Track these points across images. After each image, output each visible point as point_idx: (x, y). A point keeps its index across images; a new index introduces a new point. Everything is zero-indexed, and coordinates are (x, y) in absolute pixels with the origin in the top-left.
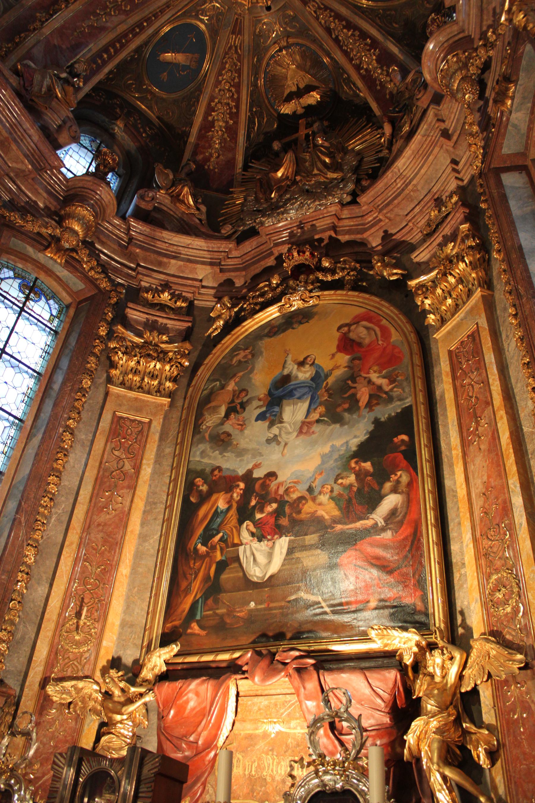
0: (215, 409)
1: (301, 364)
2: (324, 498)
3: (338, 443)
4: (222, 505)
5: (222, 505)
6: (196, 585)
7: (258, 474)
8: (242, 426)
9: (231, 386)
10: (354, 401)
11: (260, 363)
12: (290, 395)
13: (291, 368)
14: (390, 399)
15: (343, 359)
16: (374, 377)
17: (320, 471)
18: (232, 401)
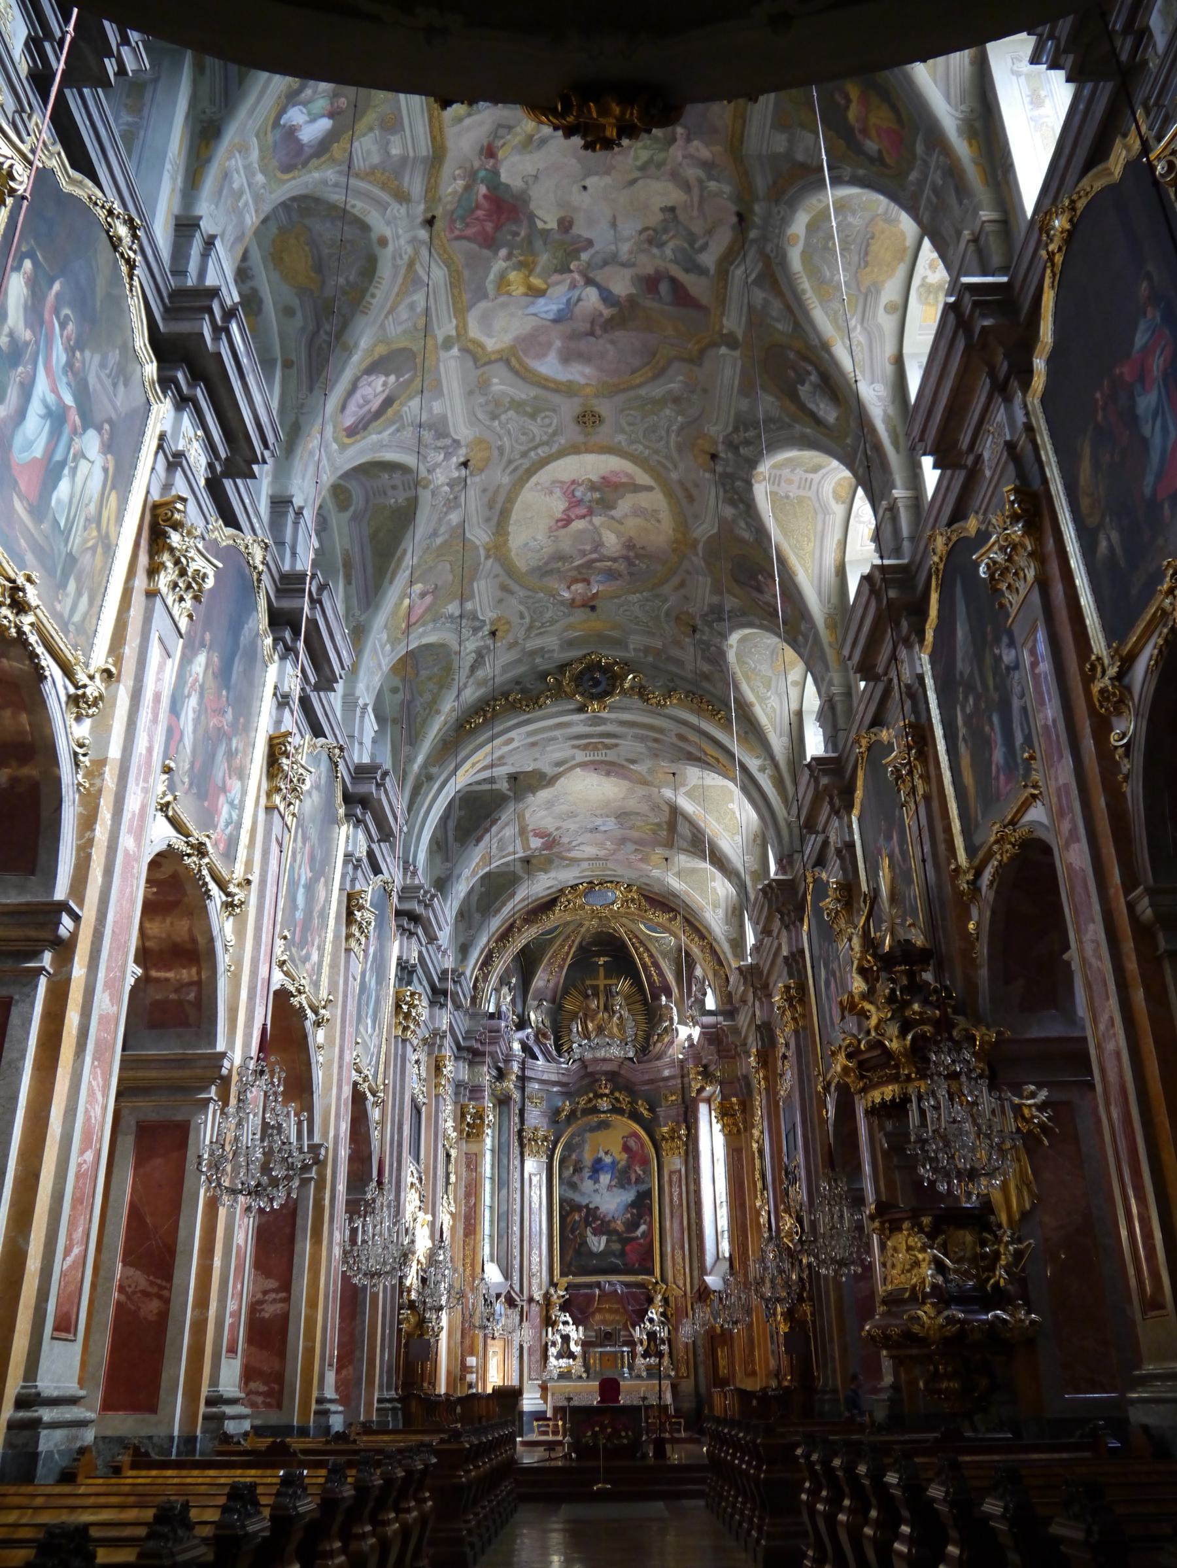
0: (568, 1168)
1: (606, 1153)
2: (619, 1222)
3: (624, 1198)
4: (577, 1218)
5: (577, 1218)
6: (571, 1252)
7: (591, 1206)
8: (582, 1180)
9: (574, 1157)
10: (629, 1179)
11: (587, 1147)
12: (602, 1169)
13: (601, 1154)
14: (643, 1182)
15: (625, 1156)
16: (637, 1169)
17: (616, 1210)
18: (575, 1166)
